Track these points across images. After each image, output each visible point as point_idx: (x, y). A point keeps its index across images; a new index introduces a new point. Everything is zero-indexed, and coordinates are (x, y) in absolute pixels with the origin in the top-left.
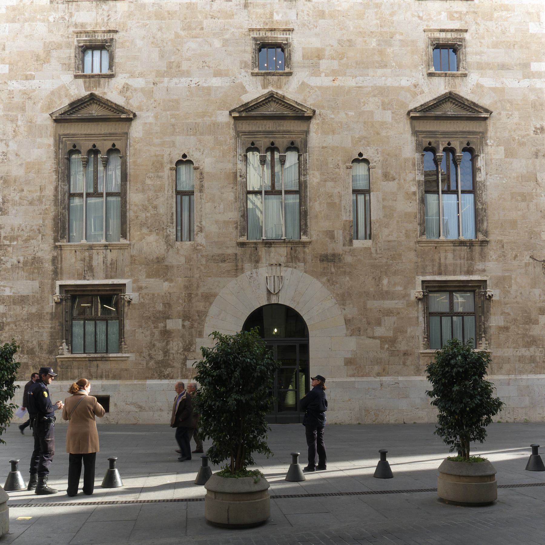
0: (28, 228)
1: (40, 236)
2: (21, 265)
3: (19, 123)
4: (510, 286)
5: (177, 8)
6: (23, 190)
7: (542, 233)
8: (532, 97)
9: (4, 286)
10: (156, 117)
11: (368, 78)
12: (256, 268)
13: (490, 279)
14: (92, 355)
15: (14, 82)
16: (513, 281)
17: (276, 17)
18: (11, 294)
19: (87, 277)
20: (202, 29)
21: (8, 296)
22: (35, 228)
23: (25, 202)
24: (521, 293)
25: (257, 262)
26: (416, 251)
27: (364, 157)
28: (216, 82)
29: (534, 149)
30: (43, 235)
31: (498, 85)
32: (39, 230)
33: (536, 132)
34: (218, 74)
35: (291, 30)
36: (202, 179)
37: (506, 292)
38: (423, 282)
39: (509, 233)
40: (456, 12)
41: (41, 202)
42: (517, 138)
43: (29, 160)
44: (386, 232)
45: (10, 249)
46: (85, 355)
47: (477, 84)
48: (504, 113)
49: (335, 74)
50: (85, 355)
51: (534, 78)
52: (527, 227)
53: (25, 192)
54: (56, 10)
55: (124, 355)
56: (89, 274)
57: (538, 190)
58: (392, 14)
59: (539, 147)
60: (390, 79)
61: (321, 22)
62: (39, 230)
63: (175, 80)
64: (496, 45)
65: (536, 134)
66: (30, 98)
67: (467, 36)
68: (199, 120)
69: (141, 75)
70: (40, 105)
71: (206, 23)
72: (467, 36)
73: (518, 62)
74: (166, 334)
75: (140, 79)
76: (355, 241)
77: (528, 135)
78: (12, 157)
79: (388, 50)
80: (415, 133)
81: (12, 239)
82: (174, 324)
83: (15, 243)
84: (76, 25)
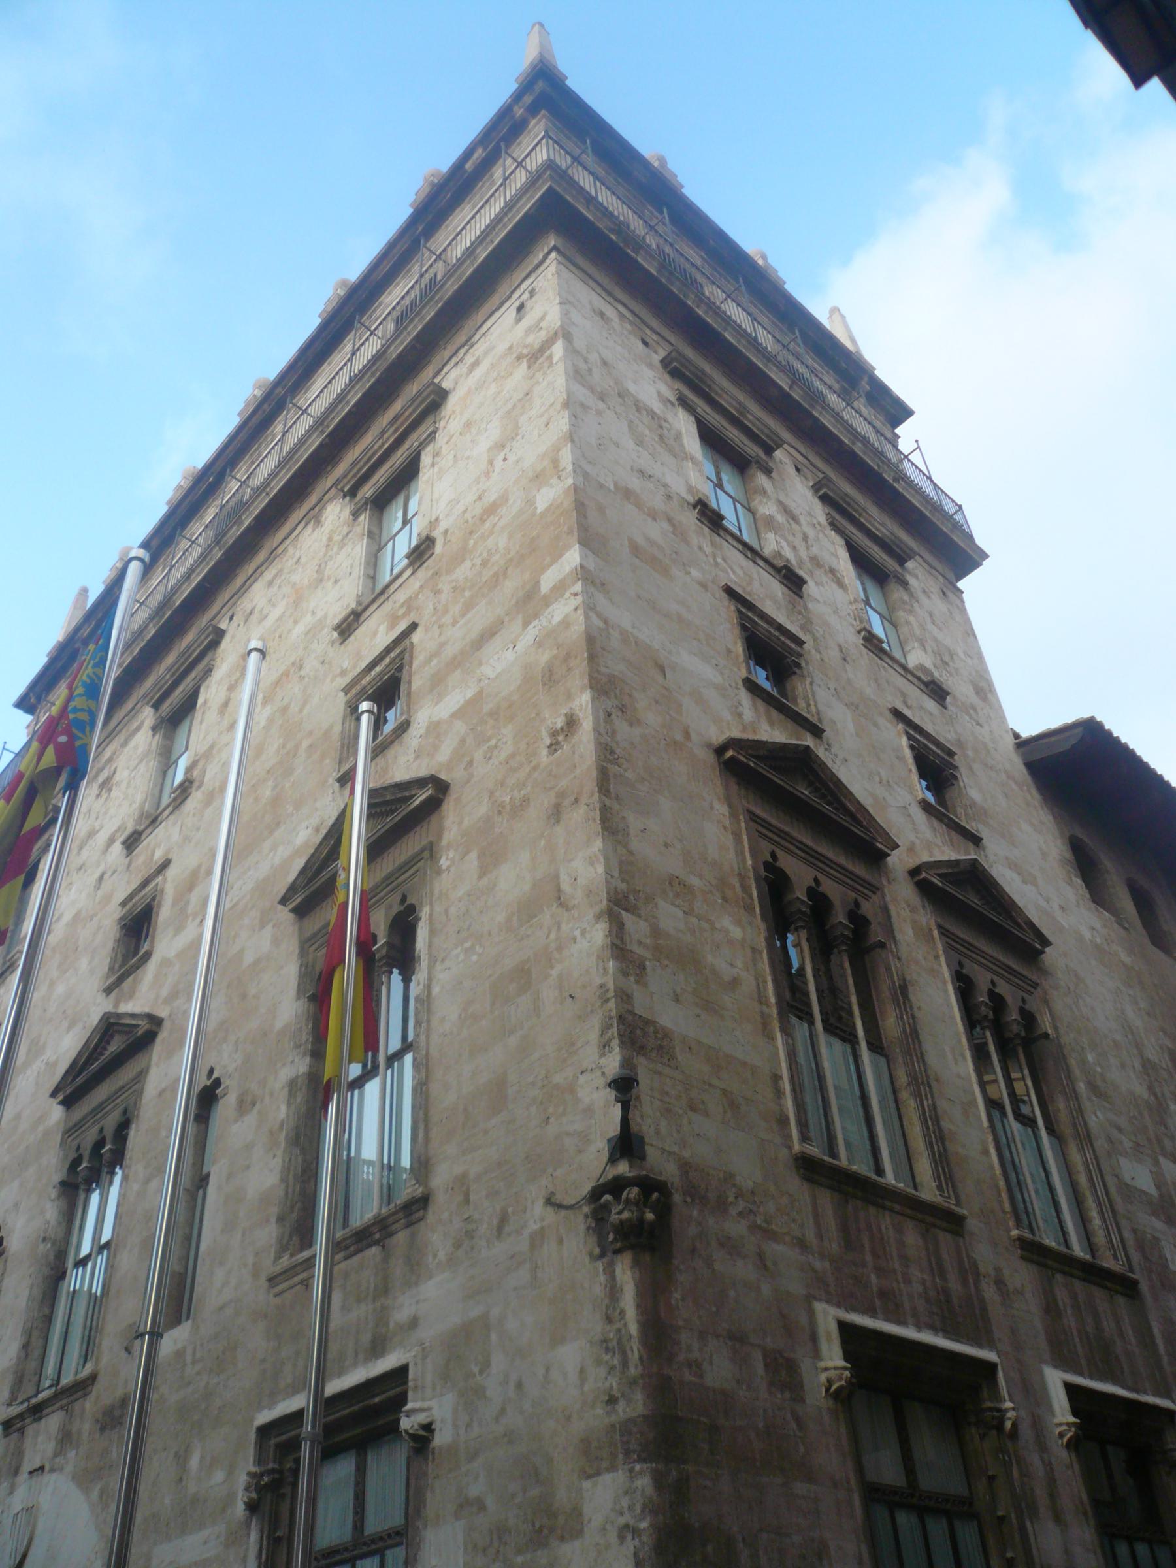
4: (485, 1366)
7: (582, 1079)
8: (545, 657)
11: (250, 873)
13: (425, 1353)
16: (494, 1337)
24: (519, 1385)
26: (266, 1316)
29: (548, 800)
31: (469, 694)
33: (553, 747)
37: (472, 1397)
39: (486, 1132)
40: (402, 605)
42: (507, 799)
44: (219, 1275)
47: (428, 728)
48: (478, 755)
51: (547, 605)
52: (533, 1084)
57: (564, 927)
59: (564, 783)
60: (281, 848)
64: (468, 607)
65: (556, 751)
67: (416, 637)
73: (513, 601)
77: (535, 768)
79: (287, 785)
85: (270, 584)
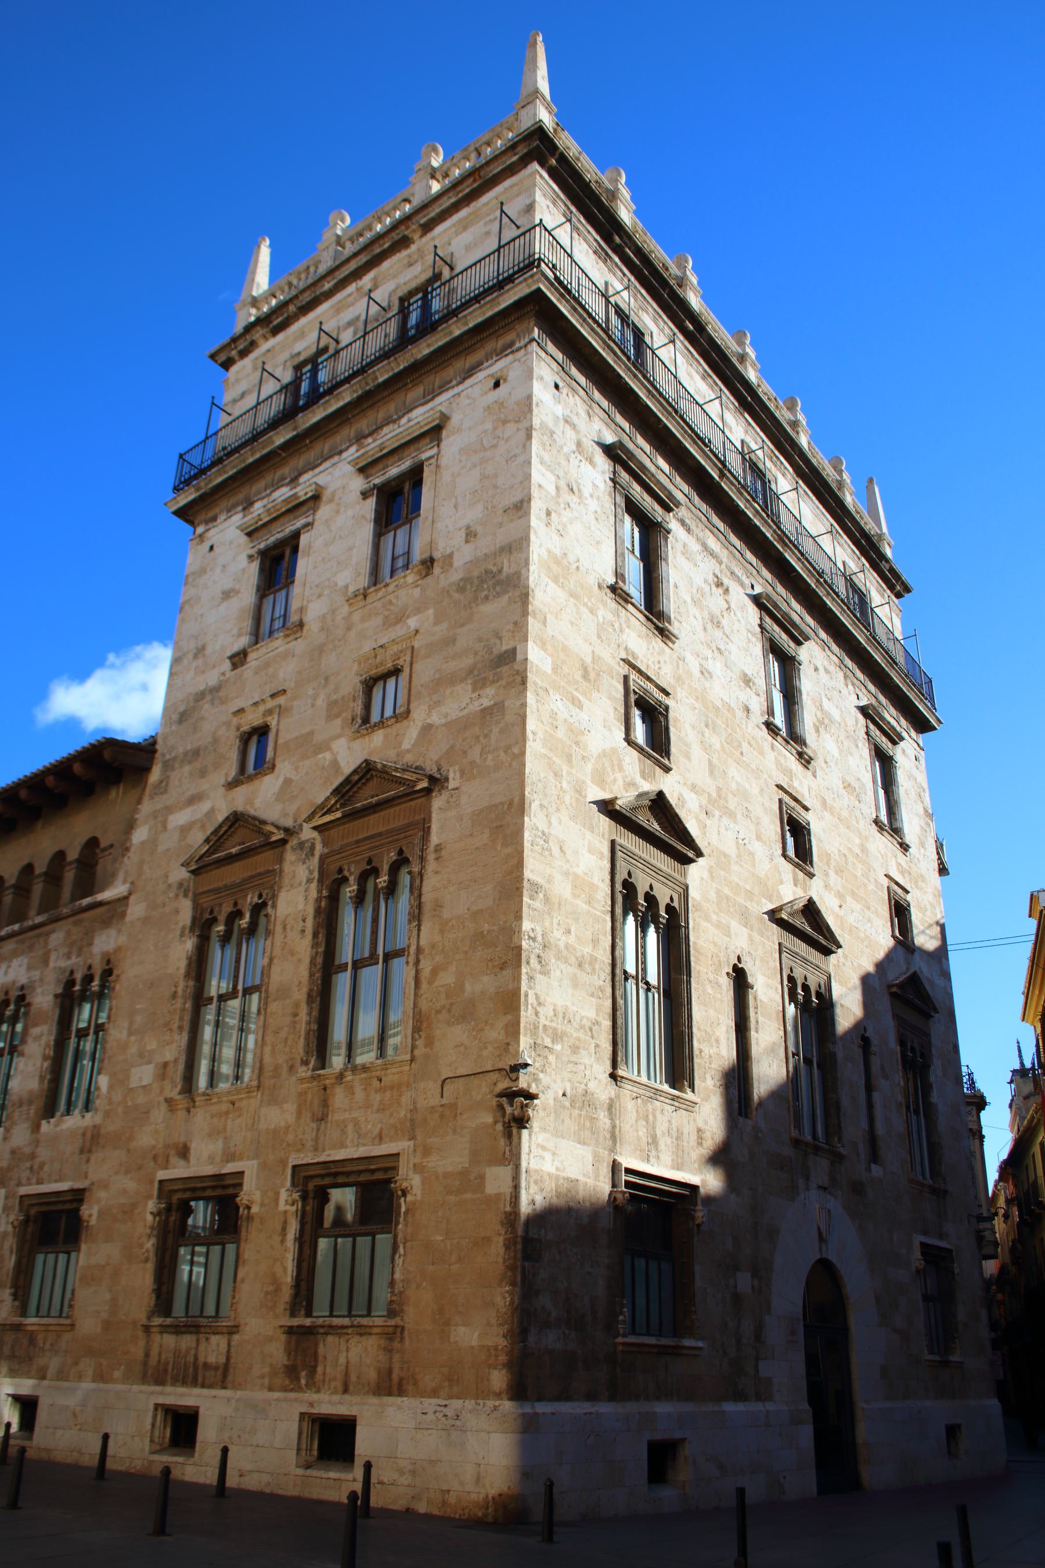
0: (578, 1018)
1: (593, 1045)
2: (567, 1104)
3: (565, 785)
5: (719, 704)
6: (569, 932)
9: (544, 1148)
10: (711, 873)
12: (808, 1189)
14: (664, 1341)
15: (558, 697)
17: (796, 784)
18: (552, 1170)
19: (651, 1159)
20: (742, 753)
21: (549, 1175)
22: (585, 1022)
23: (573, 960)
25: (807, 1178)
27: (867, 1035)
28: (757, 847)
30: (597, 1046)
32: (591, 1030)
34: (759, 838)
35: (807, 809)
36: (756, 1008)
38: (922, 1244)
41: (594, 969)
43: (579, 871)
45: (552, 1058)
46: (652, 1340)
49: (840, 896)
50: (652, 1340)
53: (572, 939)
54: (605, 605)
55: (700, 1344)
56: (653, 1153)
58: (866, 838)
61: (827, 814)
62: (591, 1030)
63: (725, 820)
66: (577, 743)
68: (748, 904)
69: (694, 788)
70: (589, 767)
71: (745, 745)
72: (909, 897)
74: (737, 1298)
75: (693, 795)
76: (873, 1166)
78: (556, 850)
80: (896, 1016)
81: (557, 1037)
82: (744, 1281)
83: (558, 1047)
84: (626, 649)
85: (827, 671)
